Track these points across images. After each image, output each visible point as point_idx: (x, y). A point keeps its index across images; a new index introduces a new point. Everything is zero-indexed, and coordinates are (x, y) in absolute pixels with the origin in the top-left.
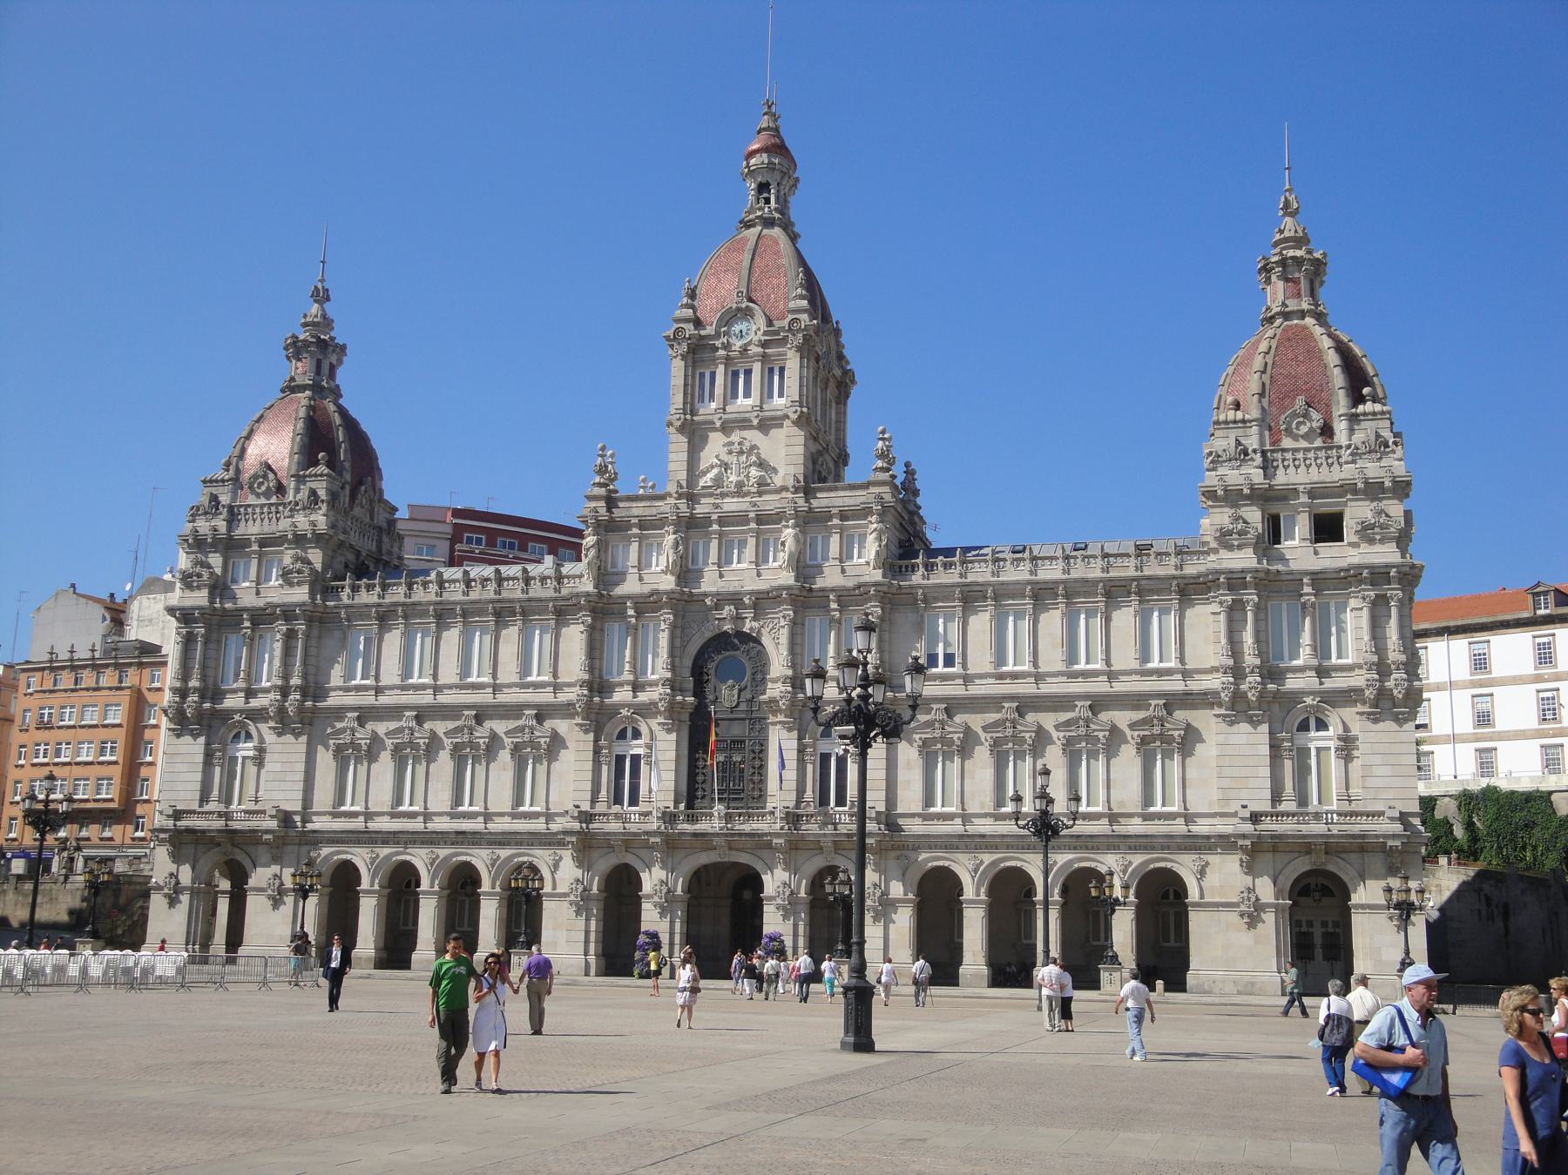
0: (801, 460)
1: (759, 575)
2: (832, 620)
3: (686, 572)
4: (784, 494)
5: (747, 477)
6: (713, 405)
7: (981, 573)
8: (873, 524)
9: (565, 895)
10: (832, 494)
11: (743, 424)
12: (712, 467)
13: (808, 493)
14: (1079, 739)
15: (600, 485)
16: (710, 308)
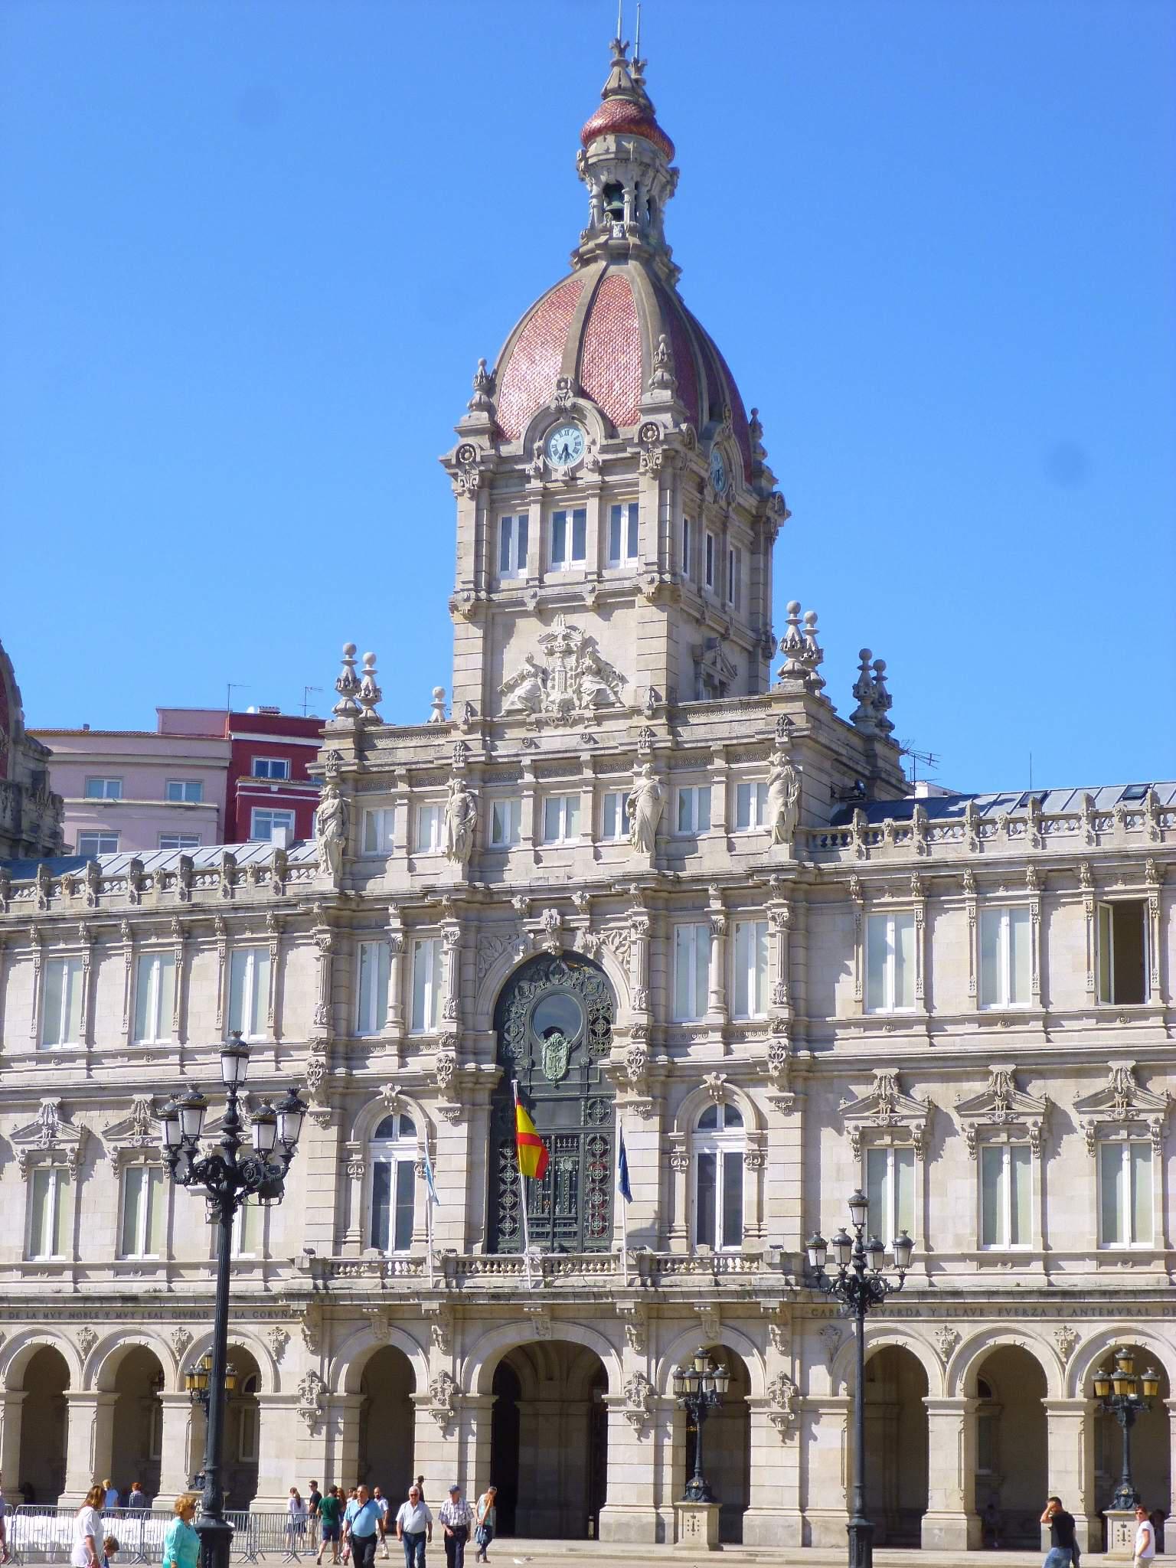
0: (662, 662)
1: (597, 856)
2: (713, 928)
3: (482, 855)
4: (636, 721)
5: (578, 692)
6: (524, 574)
7: (953, 845)
8: (775, 765)
9: (294, 1399)
10: (714, 718)
11: (571, 602)
12: (523, 677)
13: (675, 717)
14: (1115, 1126)
15: (345, 712)
16: (516, 409)
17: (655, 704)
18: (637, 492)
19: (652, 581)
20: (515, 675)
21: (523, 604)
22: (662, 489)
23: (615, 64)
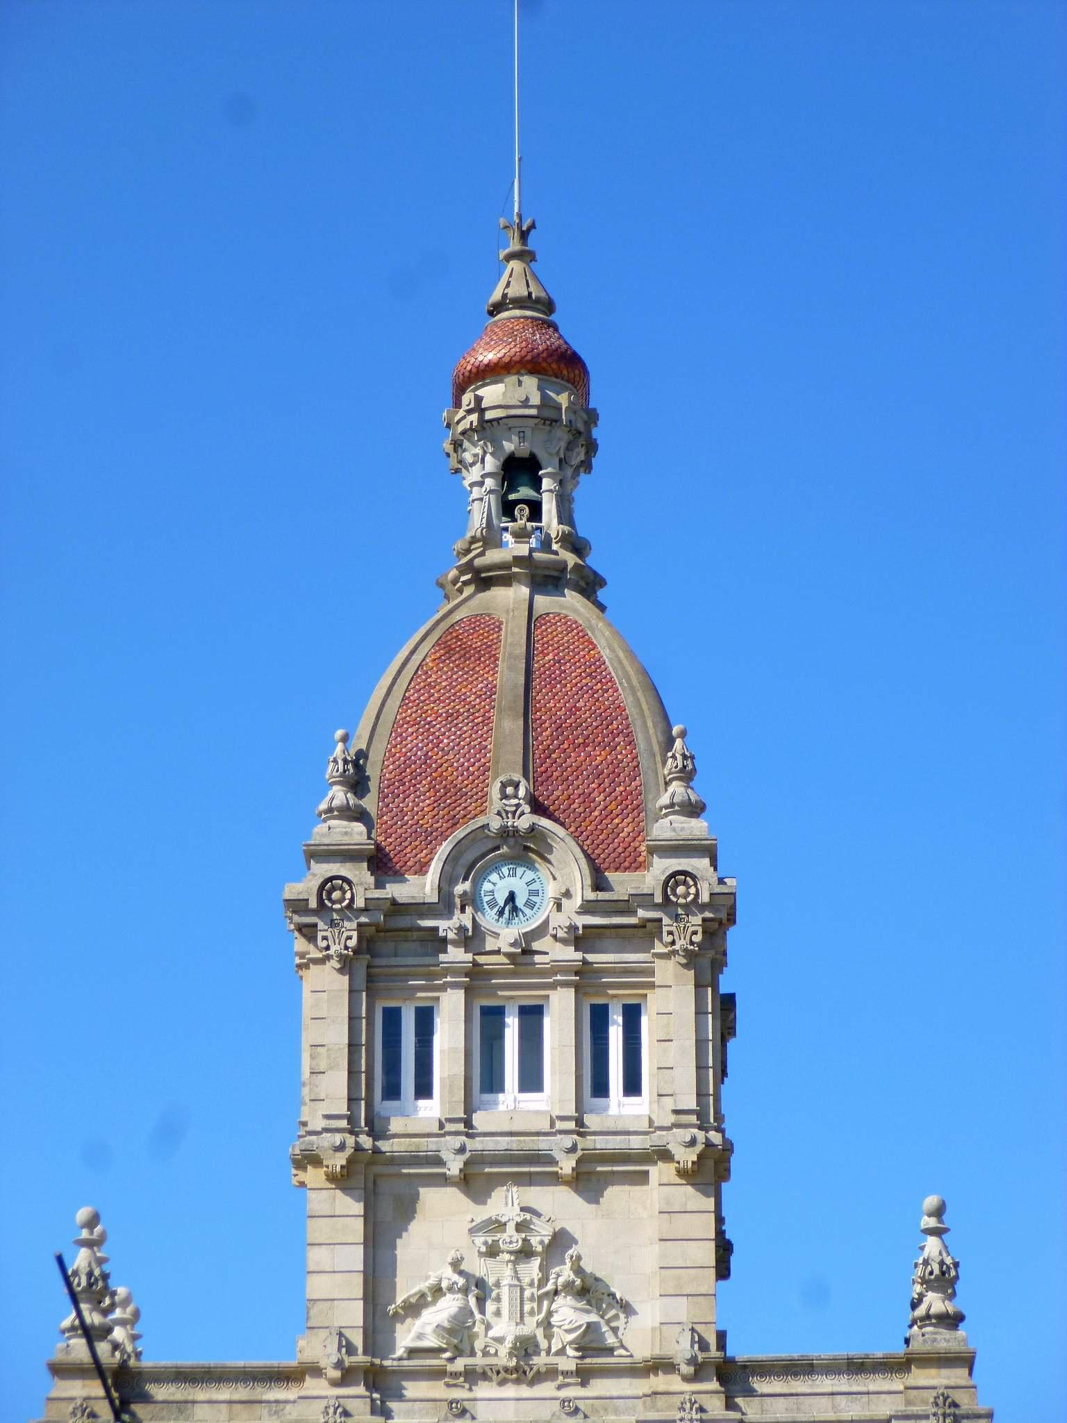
4: (660, 1382)
5: (547, 1325)
6: (429, 1111)
11: (528, 1166)
12: (438, 1291)
17: (701, 1357)
18: (652, 986)
19: (693, 1142)
20: (423, 1286)
21: (439, 1162)
22: (698, 986)
23: (509, 257)
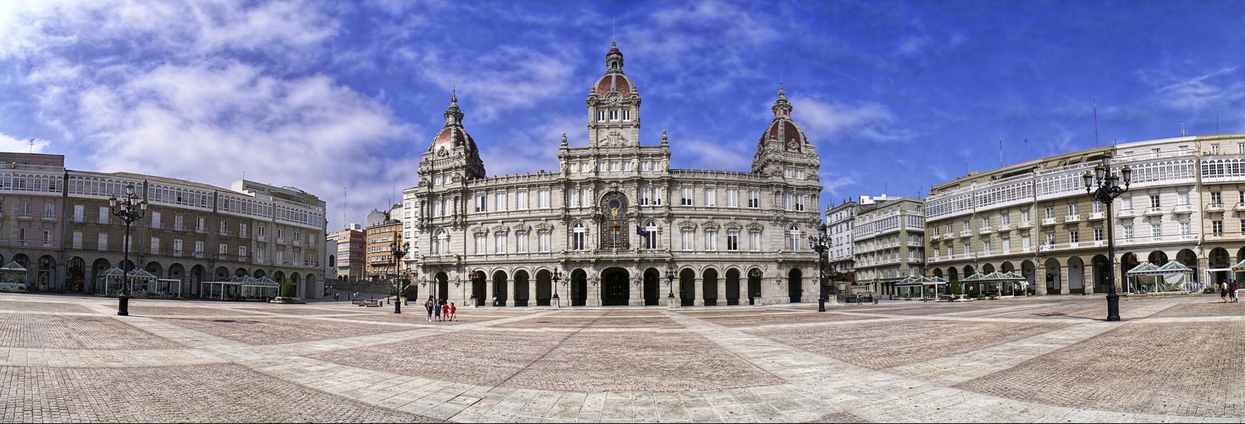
11: (615, 126)
